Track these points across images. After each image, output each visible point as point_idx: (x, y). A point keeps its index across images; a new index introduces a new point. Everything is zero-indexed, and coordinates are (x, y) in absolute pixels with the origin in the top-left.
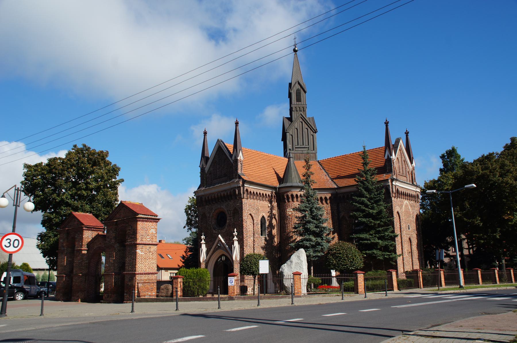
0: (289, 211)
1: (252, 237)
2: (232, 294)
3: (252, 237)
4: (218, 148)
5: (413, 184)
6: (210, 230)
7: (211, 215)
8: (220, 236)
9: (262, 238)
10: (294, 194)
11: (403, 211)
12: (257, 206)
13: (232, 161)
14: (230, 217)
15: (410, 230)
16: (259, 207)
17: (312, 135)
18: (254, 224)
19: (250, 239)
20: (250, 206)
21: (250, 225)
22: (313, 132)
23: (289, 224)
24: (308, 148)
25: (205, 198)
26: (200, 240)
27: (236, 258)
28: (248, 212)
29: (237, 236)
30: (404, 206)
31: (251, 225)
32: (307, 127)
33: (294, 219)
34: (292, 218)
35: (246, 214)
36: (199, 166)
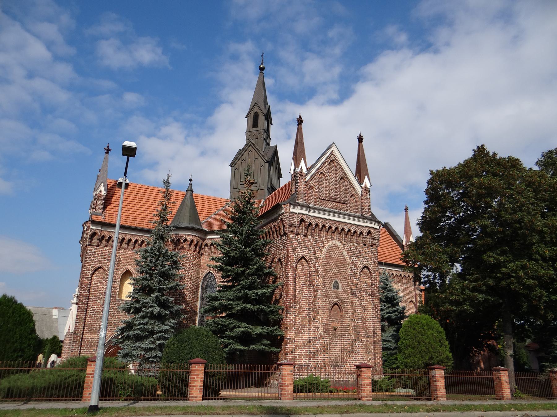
5: (363, 217)
11: (321, 257)
15: (340, 290)
19: (96, 302)
21: (99, 282)
28: (95, 265)
30: (324, 249)
31: (102, 282)
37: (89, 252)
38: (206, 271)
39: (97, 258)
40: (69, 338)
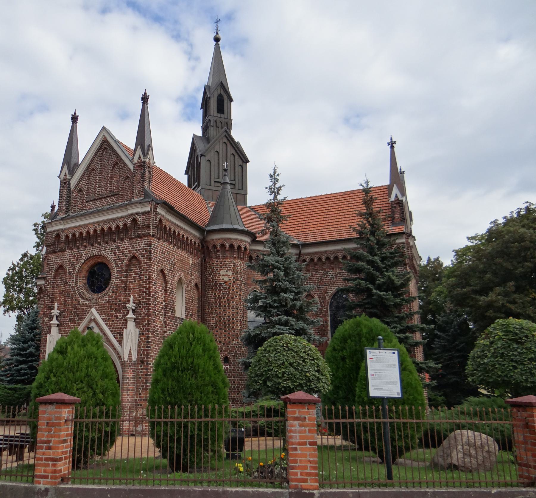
0: (224, 274)
1: (161, 315)
2: (305, 481)
3: (161, 315)
4: (102, 144)
6: (72, 298)
7: (77, 268)
8: (93, 310)
9: (177, 320)
10: (236, 244)
12: (173, 258)
13: (131, 167)
14: (121, 271)
16: (176, 260)
17: (240, 165)
18: (166, 291)
19: (159, 319)
20: (163, 253)
22: (243, 162)
23: (224, 298)
24: (234, 185)
25: (67, 236)
26: (47, 319)
27: (130, 356)
29: (134, 311)
32: (233, 151)
33: (233, 290)
34: (229, 288)
35: (155, 268)
36: (59, 177)
37: (154, 247)
38: (251, 289)
39: (159, 256)
40: (132, 369)
